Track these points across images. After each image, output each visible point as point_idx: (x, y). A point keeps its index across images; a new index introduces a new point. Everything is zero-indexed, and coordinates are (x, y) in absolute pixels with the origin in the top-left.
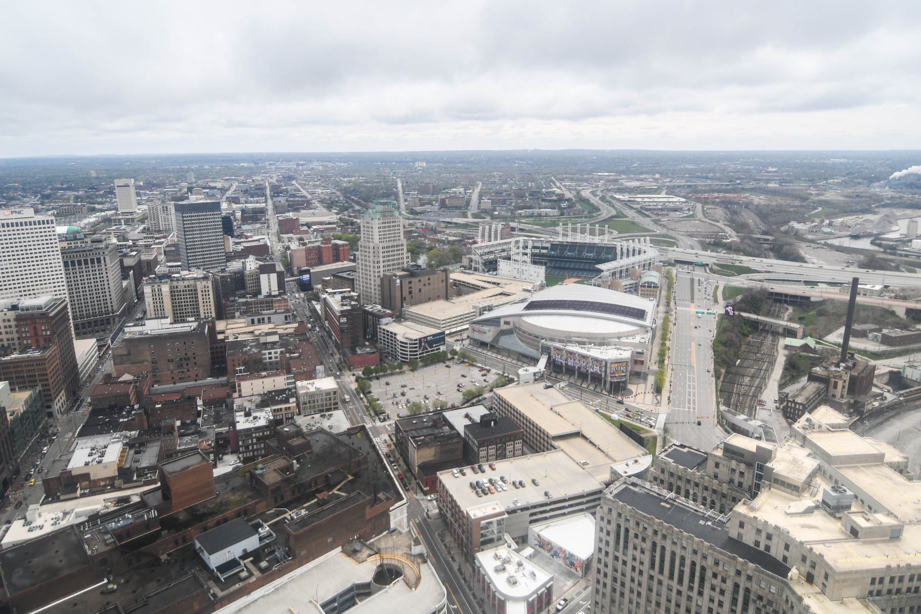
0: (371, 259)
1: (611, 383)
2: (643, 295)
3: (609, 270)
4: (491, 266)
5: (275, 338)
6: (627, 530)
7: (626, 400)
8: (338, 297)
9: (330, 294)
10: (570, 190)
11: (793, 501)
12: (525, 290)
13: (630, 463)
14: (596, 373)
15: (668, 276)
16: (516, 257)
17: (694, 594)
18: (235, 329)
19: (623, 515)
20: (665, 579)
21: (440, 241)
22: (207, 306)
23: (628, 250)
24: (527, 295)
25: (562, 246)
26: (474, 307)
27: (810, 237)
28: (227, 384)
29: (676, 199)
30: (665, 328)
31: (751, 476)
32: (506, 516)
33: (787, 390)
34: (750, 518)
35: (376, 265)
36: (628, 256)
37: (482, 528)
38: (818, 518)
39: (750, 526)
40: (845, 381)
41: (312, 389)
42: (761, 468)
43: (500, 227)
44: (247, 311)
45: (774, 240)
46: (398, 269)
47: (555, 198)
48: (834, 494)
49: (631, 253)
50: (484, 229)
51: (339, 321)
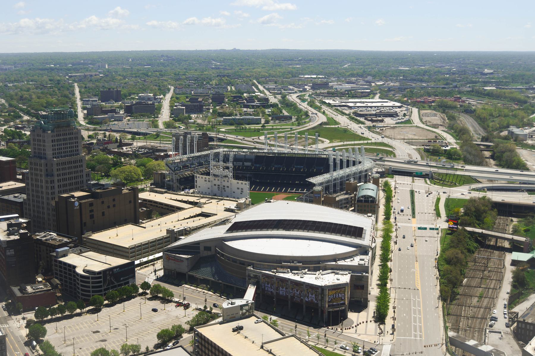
1: (329, 312)
3: (321, 184)
7: (346, 332)
10: (274, 94)
14: (312, 302)
15: (387, 189)
21: (125, 155)
23: (341, 161)
27: (530, 142)
29: (391, 104)
30: (386, 248)
33: (516, 309)
35: (49, 185)
36: (341, 168)
45: (496, 146)
46: (77, 190)
47: (256, 103)
49: (345, 164)
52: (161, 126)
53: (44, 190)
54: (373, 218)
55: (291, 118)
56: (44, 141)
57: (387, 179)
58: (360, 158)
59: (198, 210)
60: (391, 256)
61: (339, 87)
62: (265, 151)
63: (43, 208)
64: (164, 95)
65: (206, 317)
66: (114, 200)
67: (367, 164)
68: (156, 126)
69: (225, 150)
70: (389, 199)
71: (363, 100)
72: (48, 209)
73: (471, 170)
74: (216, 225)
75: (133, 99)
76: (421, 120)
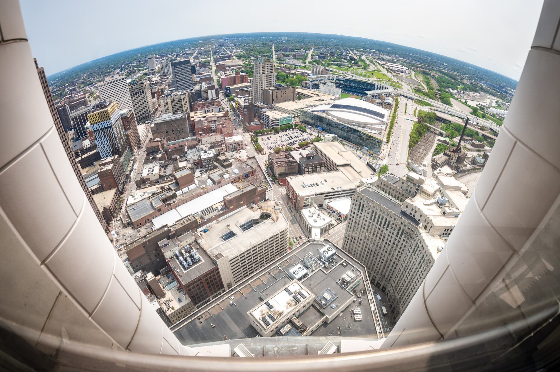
2: (384, 108)
5: (215, 119)
8: (243, 99)
16: (328, 84)
17: (384, 230)
18: (197, 116)
20: (375, 223)
21: (292, 74)
22: (186, 105)
25: (350, 81)
28: (196, 139)
43: (321, 69)
44: (203, 106)
47: (348, 58)
50: (313, 69)
52: (307, 63)
54: (389, 111)
59: (319, 98)
60: (394, 127)
68: (305, 63)
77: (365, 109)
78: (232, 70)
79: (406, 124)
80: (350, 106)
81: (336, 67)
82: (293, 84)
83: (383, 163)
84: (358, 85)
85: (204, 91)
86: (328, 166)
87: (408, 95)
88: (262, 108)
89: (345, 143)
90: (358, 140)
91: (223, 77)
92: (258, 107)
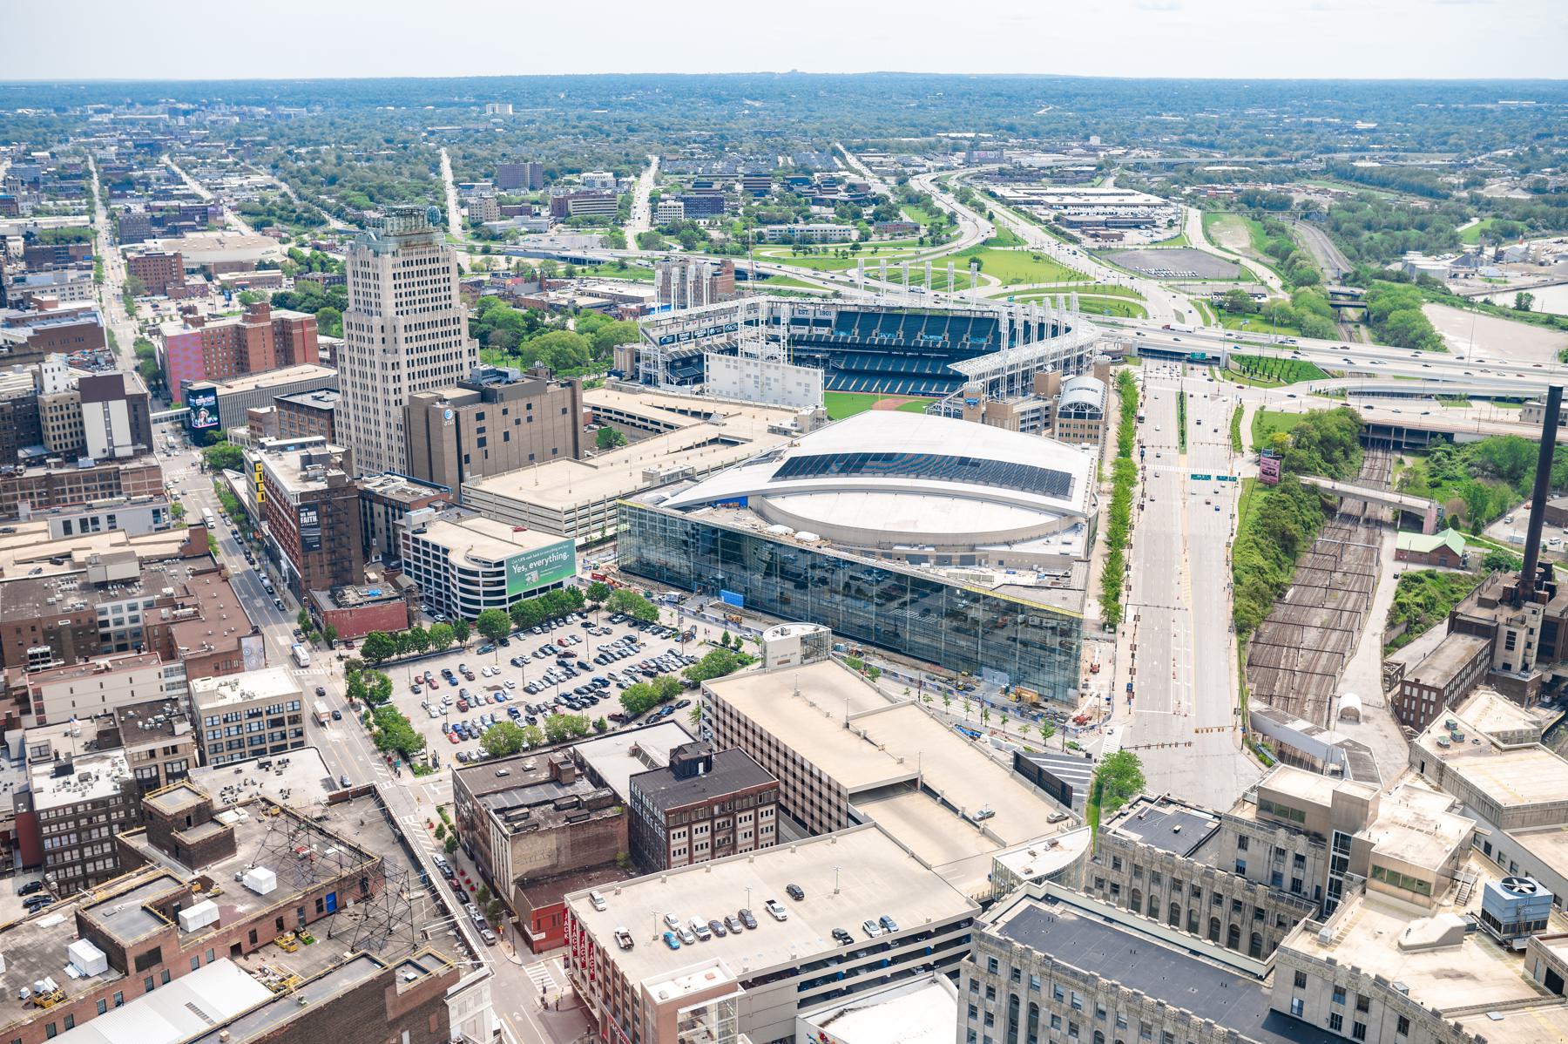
0: (376, 359)
2: (1065, 437)
4: (689, 369)
6: (1034, 1010)
8: (294, 458)
9: (270, 449)
11: (1417, 916)
12: (773, 430)
13: (1039, 848)
19: (1024, 974)
21: (555, 308)
23: (1027, 325)
24: (780, 442)
25: (868, 318)
26: (647, 476)
29: (1141, 198)
31: (1321, 863)
32: (741, 992)
33: (1399, 656)
34: (1319, 963)
35: (391, 373)
36: (1027, 341)
37: (683, 1026)
38: (1476, 954)
39: (1319, 981)
40: (1531, 631)
41: (232, 698)
42: (1343, 842)
44: (49, 495)
46: (449, 381)
48: (1507, 896)
49: (1034, 333)
50: (667, 276)
51: (297, 521)
53: (379, 383)
54: (1094, 451)
55: (917, 229)
56: (377, 277)
57: (1125, 366)
58: (1067, 319)
60: (1133, 536)
61: (1026, 161)
62: (860, 302)
63: (377, 423)
64: (638, 176)
65: (725, 663)
66: (529, 407)
67: (1085, 333)
69: (772, 298)
70: (1130, 412)
71: (1078, 190)
72: (388, 425)
73: (1316, 351)
74: (751, 463)
75: (570, 183)
76: (1208, 237)
77: (964, 461)
78: (224, 289)
79: (1195, 517)
80: (877, 457)
81: (785, 251)
82: (564, 363)
83: (1104, 745)
84: (910, 334)
85: (59, 405)
86: (802, 806)
87: (1187, 345)
88: (401, 508)
89: (876, 663)
90: (944, 633)
91: (173, 328)
92: (380, 499)
